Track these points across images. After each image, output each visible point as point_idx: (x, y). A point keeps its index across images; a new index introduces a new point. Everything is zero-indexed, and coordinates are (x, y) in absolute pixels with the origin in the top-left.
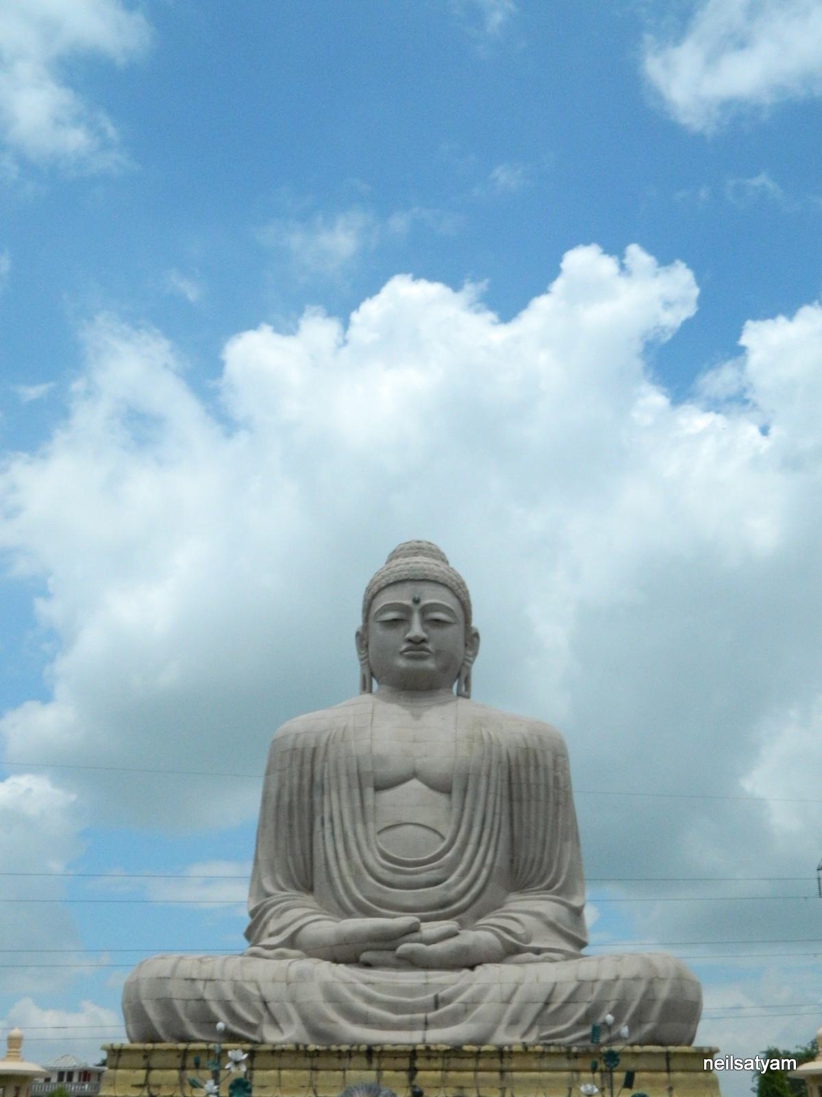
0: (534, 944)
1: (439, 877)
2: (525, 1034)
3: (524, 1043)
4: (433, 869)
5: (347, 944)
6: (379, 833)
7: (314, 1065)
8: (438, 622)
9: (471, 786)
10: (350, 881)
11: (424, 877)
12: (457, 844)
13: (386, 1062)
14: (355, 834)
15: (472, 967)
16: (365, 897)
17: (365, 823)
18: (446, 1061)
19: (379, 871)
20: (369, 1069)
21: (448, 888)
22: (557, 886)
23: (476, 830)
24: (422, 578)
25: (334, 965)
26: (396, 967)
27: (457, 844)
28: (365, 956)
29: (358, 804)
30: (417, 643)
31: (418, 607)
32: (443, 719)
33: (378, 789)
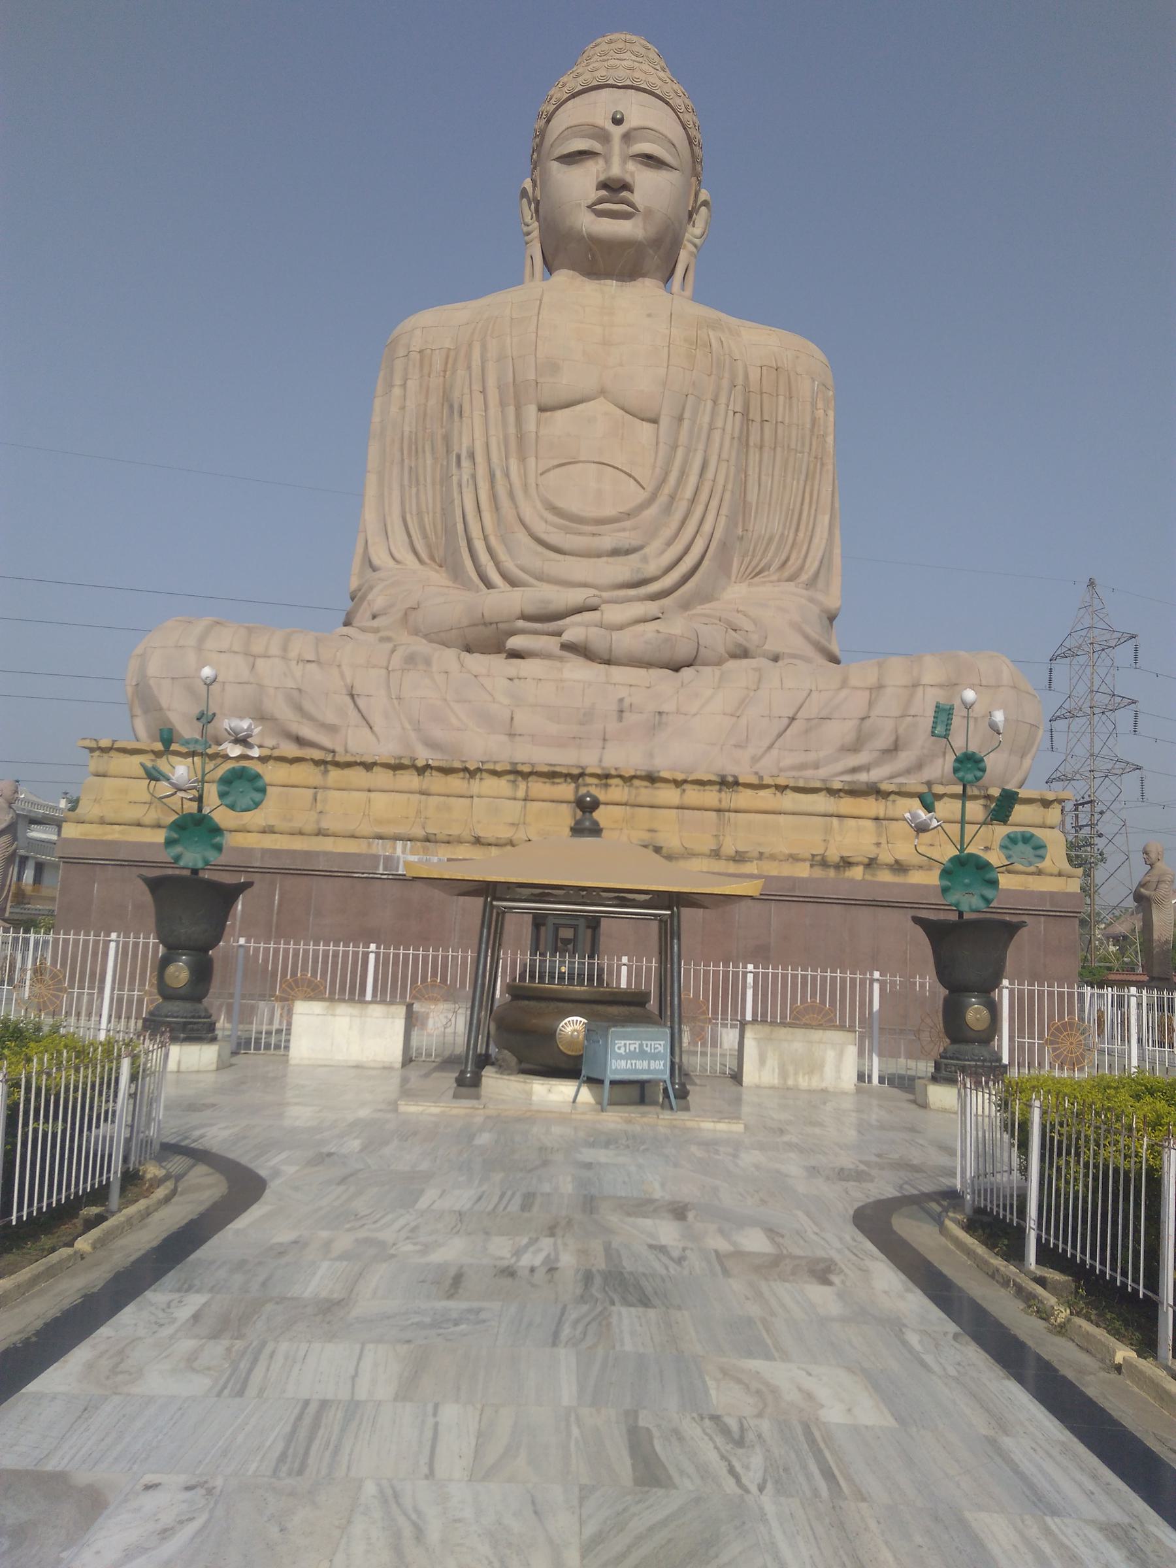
0: (771, 646)
1: (635, 543)
2: (755, 760)
3: (756, 773)
4: (624, 530)
5: (485, 624)
6: (541, 474)
7: (424, 787)
8: (650, 160)
9: (687, 415)
10: (493, 541)
11: (607, 542)
12: (663, 498)
13: (539, 788)
14: (507, 475)
15: (677, 669)
16: (517, 566)
17: (523, 459)
18: (634, 791)
19: (540, 528)
20: (515, 799)
21: (645, 560)
22: (804, 577)
23: (693, 479)
24: (628, 83)
25: (464, 654)
26: (561, 659)
27: (663, 498)
28: (514, 642)
29: (512, 430)
30: (615, 188)
31: (617, 132)
32: (649, 315)
33: (542, 409)
